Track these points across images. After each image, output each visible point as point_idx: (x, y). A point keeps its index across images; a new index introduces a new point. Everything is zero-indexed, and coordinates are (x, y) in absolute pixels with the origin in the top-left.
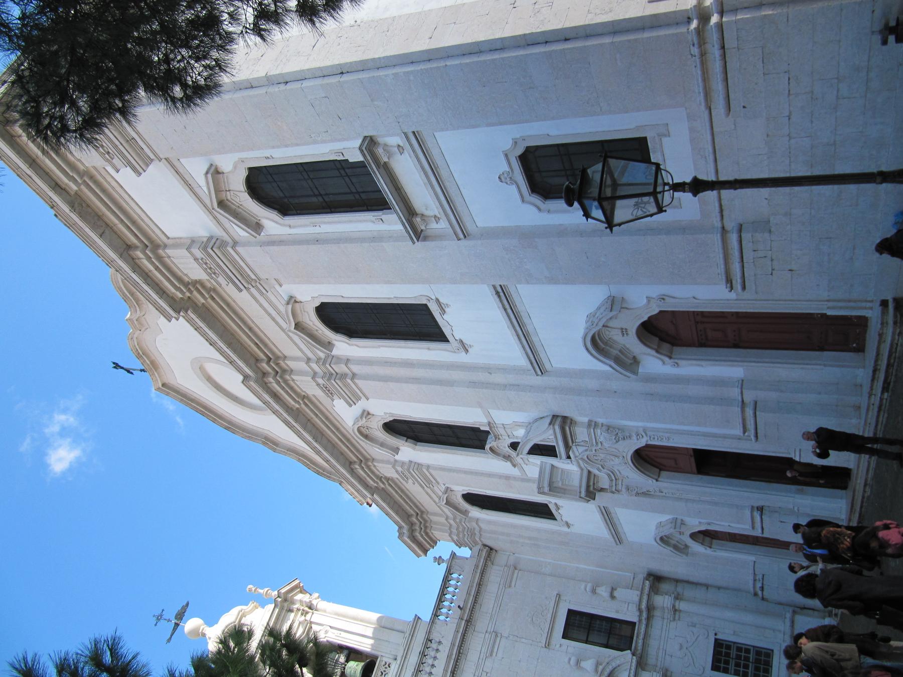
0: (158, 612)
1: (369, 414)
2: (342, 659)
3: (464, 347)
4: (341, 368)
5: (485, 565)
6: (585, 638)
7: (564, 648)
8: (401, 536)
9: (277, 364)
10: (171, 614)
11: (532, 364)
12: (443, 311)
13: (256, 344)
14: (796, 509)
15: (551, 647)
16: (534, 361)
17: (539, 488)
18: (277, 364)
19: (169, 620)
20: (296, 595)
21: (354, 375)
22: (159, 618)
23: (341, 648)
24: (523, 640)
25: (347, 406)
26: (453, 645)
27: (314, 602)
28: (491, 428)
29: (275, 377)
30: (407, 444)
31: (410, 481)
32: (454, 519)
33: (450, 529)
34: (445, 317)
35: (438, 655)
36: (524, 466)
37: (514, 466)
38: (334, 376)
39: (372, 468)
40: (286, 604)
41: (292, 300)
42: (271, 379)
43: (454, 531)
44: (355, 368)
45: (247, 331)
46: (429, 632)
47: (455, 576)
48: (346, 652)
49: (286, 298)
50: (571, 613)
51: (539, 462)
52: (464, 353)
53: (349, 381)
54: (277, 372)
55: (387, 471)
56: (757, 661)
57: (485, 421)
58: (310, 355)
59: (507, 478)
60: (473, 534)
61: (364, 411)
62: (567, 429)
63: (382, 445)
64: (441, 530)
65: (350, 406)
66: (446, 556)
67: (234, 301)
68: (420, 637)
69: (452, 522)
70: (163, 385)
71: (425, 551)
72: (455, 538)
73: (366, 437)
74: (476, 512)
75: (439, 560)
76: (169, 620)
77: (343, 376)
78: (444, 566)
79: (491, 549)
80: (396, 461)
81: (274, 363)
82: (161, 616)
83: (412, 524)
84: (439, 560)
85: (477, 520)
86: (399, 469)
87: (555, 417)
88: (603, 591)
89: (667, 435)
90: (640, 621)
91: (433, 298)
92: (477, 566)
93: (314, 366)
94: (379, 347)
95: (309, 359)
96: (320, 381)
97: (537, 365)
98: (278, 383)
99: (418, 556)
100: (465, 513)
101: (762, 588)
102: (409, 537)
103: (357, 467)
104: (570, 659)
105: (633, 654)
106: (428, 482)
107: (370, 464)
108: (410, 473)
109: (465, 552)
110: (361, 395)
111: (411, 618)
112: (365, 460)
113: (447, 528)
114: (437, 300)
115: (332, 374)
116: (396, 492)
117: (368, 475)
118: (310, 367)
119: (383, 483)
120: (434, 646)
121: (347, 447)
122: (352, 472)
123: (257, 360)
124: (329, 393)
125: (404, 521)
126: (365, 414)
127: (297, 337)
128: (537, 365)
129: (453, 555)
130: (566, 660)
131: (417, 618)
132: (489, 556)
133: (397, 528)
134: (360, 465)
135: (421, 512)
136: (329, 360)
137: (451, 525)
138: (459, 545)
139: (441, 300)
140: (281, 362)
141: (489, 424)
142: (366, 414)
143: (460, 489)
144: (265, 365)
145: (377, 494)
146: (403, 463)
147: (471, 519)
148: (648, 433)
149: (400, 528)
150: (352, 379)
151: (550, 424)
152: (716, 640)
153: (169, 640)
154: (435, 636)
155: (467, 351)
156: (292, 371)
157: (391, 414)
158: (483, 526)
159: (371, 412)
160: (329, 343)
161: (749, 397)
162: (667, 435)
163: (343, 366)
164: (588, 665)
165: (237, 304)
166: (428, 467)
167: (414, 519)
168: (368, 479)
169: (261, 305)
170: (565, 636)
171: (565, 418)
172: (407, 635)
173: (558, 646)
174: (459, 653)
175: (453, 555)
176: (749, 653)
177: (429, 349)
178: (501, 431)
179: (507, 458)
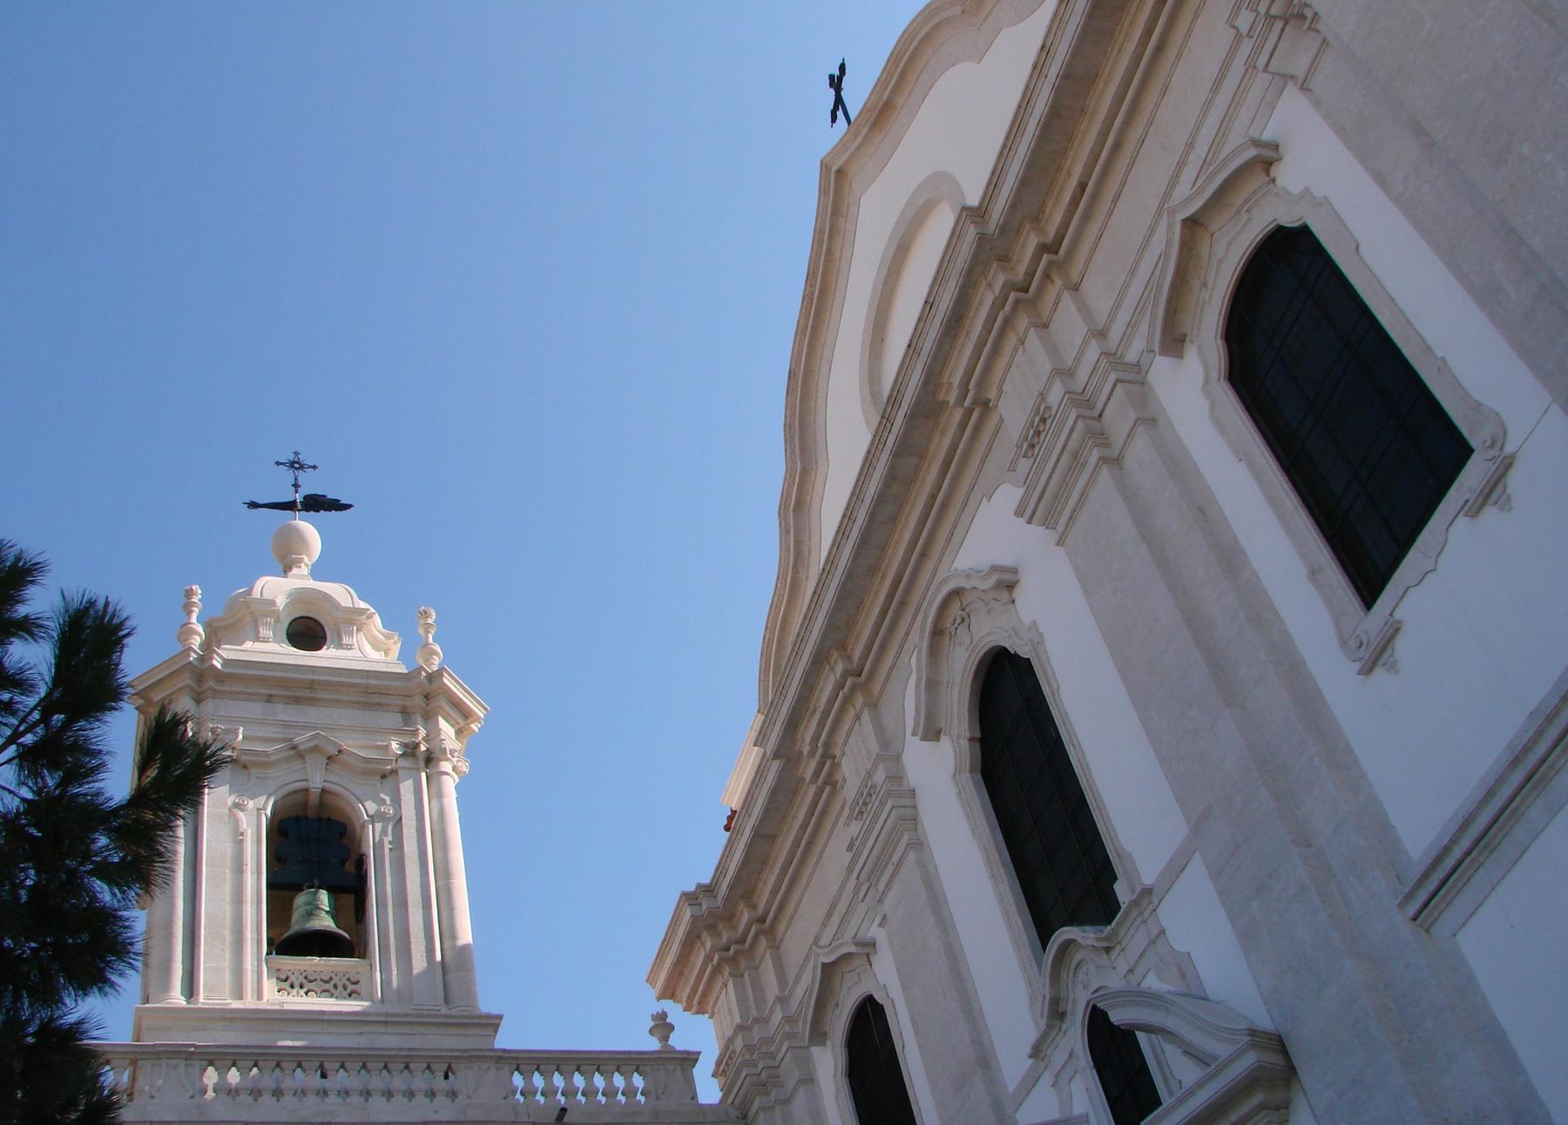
0: (306, 459)
1: (1010, 587)
3: (1376, 656)
4: (1119, 418)
8: (689, 898)
9: (1047, 276)
10: (312, 484)
11: (1426, 875)
12: (1474, 509)
13: (1082, 186)
16: (1450, 862)
18: (1047, 276)
19: (296, 486)
21: (1115, 462)
22: (296, 465)
25: (1014, 506)
27: (446, 766)
28: (1135, 903)
29: (1009, 287)
30: (965, 744)
31: (856, 827)
32: (788, 1019)
33: (756, 1020)
34: (1462, 521)
35: (420, 1099)
36: (1047, 1078)
37: (1037, 1052)
38: (1088, 413)
39: (851, 713)
40: (418, 701)
41: (1265, 160)
42: (1000, 280)
43: (756, 1034)
44: (1140, 451)
45: (1117, 123)
47: (638, 1081)
49: (1267, 136)
51: (1078, 1110)
52: (1357, 666)
53: (1095, 455)
54: (1027, 291)
55: (856, 759)
57: (1148, 877)
58: (1116, 331)
59: (984, 1060)
60: (762, 1087)
61: (1014, 571)
62: (1257, 1098)
63: (932, 686)
64: (742, 1000)
65: (1019, 513)
66: (678, 1041)
67: (1179, 56)
68: (450, 1041)
69: (778, 1016)
70: (840, 173)
71: (669, 992)
73: (937, 633)
74: (829, 1063)
75: (662, 1026)
76: (296, 486)
77: (1099, 437)
78: (653, 1044)
80: (898, 758)
81: (1050, 264)
82: (302, 467)
84: (662, 1026)
85: (809, 1080)
86: (880, 776)
87: (1278, 1044)
91: (1508, 449)
93: (1093, 352)
94: (1244, 456)
95: (1102, 334)
96: (1056, 394)
97: (1445, 878)
98: (999, 303)
99: (651, 979)
100: (818, 1035)
102: (694, 919)
103: (839, 668)
106: (872, 874)
107: (859, 700)
108: (882, 804)
109: (708, 1090)
110: (1060, 528)
111: (486, 1004)
112: (861, 681)
113: (754, 1013)
114: (1508, 464)
115: (1092, 408)
116: (805, 826)
117: (826, 714)
118: (1082, 350)
119: (817, 774)
120: (440, 1083)
121: (884, 612)
122: (819, 661)
123: (1037, 220)
124: (1032, 441)
125: (731, 888)
126: (1009, 577)
127: (1167, 237)
128: (1445, 878)
131: (492, 1023)
134: (846, 674)
135: (768, 927)
136: (1131, 377)
138: (722, 1069)
139: (1514, 479)
140: (1058, 283)
141: (1148, 891)
142: (1007, 582)
143: (883, 978)
144: (1032, 242)
145: (782, 772)
146: (897, 777)
147: (805, 1064)
150: (1104, 460)
153: (253, 505)
154: (464, 1079)
155: (1367, 670)
156: (1046, 326)
157: (1038, 643)
158: (800, 1101)
159: (1018, 593)
160: (1182, 340)
163: (1133, 415)
165: (1175, 65)
166: (918, 844)
167: (745, 917)
168: (817, 716)
169: (1207, 105)
171: (1291, 1071)
172: (444, 1010)
177: (1313, 574)
178: (1135, 940)
179: (1057, 1013)
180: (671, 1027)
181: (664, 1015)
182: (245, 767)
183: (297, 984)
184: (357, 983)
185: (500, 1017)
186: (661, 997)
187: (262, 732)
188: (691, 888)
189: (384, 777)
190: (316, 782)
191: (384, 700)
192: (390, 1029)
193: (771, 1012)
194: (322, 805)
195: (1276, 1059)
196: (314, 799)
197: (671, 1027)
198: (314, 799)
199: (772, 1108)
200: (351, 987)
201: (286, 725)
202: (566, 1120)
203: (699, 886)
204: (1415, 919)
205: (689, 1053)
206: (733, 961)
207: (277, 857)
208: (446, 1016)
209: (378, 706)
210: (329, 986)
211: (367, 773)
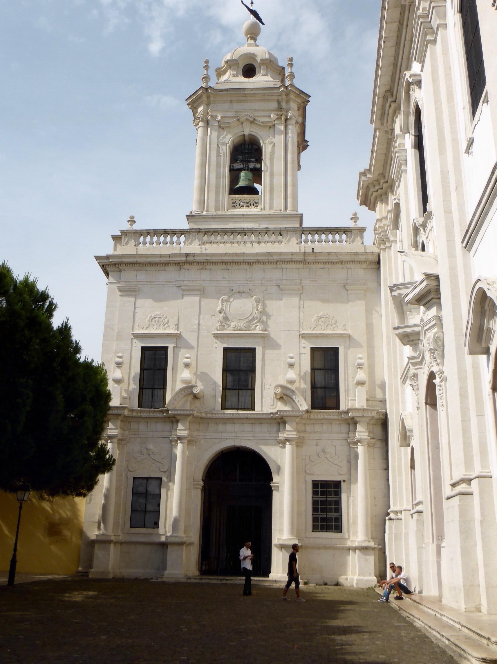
2: (251, 166)
5: (361, 262)
6: (315, 367)
7: (303, 351)
14: (424, 546)
15: (303, 341)
17: (394, 286)
19: (252, 3)
20: (295, 101)
23: (259, 160)
24: (301, 313)
26: (280, 254)
30: (413, 137)
33: (383, 218)
46: (287, 230)
47: (344, 237)
48: (258, 166)
50: (335, 350)
56: (329, 520)
66: (360, 224)
72: (377, 226)
75: (355, 218)
78: (350, 224)
79: (379, 263)
83: (378, 181)
84: (355, 218)
88: (361, 375)
89: (444, 403)
90: (340, 413)
92: (356, 254)
101: (390, 519)
104: (291, 358)
105: (307, 411)
129: (362, 230)
130: (291, 355)
132: (371, 263)
133: (368, 167)
137: (386, 218)
145: (379, 133)
148: (443, 383)
149: (369, 171)
151: (426, 275)
152: (340, 482)
161: (475, 486)
162: (444, 403)
164: (292, 374)
166: (406, 171)
167: (382, 181)
170: (314, 350)
173: (304, 345)
174: (277, 262)
175: (362, 230)
176: (335, 512)
180: (358, 218)
181: (356, 214)
182: (223, 129)
183: (238, 204)
184: (257, 203)
185: (302, 214)
186: (361, 205)
187: (229, 114)
188: (363, 170)
189: (270, 127)
190: (247, 132)
191: (270, 98)
192: (265, 219)
193: (387, 215)
194: (250, 139)
195: (434, 283)
196: (247, 139)
197: (358, 218)
198: (247, 139)
199: (385, 249)
200: (255, 204)
201: (237, 111)
202: (315, 251)
203: (365, 170)
204: (465, 248)
205: (362, 227)
206: (381, 196)
207: (233, 159)
208: (284, 214)
209: (269, 100)
210: (249, 204)
211: (265, 126)
